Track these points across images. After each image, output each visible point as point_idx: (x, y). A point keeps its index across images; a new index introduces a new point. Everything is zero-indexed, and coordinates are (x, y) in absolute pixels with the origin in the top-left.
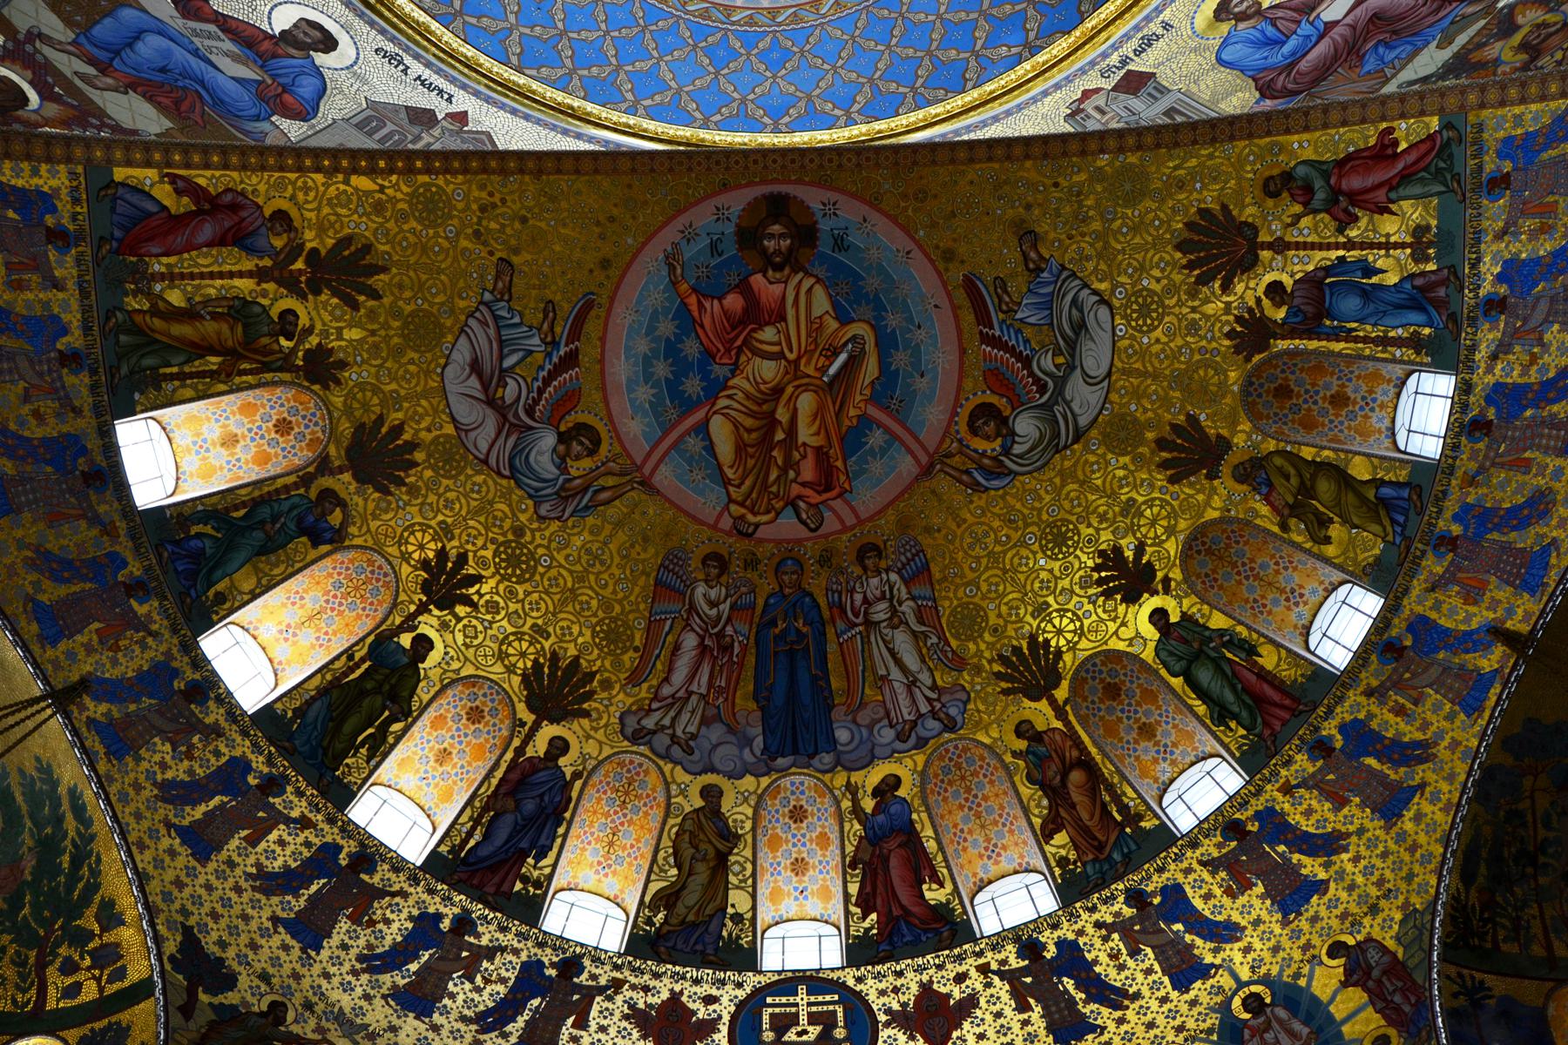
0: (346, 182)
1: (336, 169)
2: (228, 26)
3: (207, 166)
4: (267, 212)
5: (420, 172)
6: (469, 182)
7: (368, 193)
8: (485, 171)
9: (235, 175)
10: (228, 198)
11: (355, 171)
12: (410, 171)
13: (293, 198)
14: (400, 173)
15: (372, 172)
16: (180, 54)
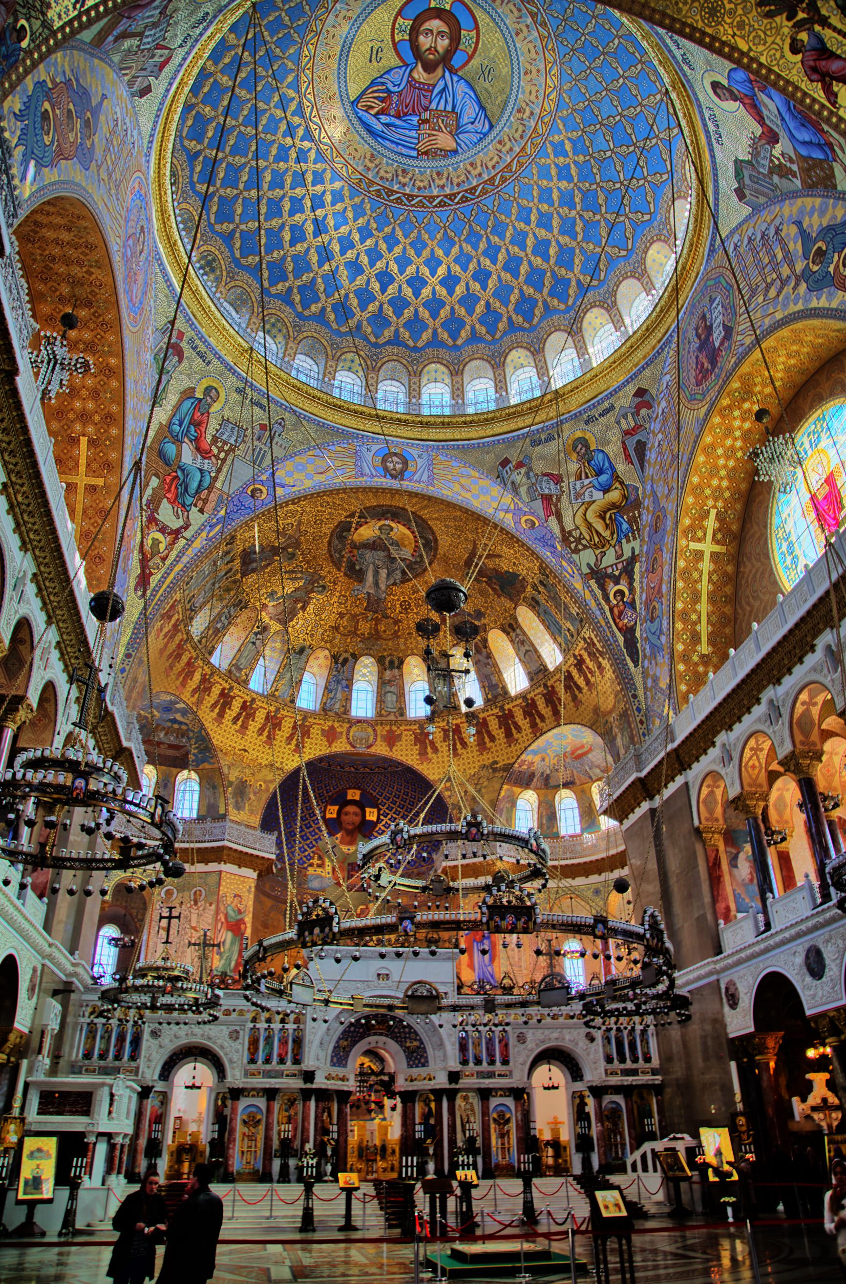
0: (750, 49)
1: (752, 60)
2: (760, 120)
3: (814, 100)
4: (800, 56)
5: (709, 35)
6: (685, 17)
7: (743, 37)
8: (674, 20)
9: (803, 87)
10: (814, 77)
11: (742, 54)
12: (714, 38)
13: (782, 57)
14: (719, 40)
15: (734, 48)
16: (791, 125)
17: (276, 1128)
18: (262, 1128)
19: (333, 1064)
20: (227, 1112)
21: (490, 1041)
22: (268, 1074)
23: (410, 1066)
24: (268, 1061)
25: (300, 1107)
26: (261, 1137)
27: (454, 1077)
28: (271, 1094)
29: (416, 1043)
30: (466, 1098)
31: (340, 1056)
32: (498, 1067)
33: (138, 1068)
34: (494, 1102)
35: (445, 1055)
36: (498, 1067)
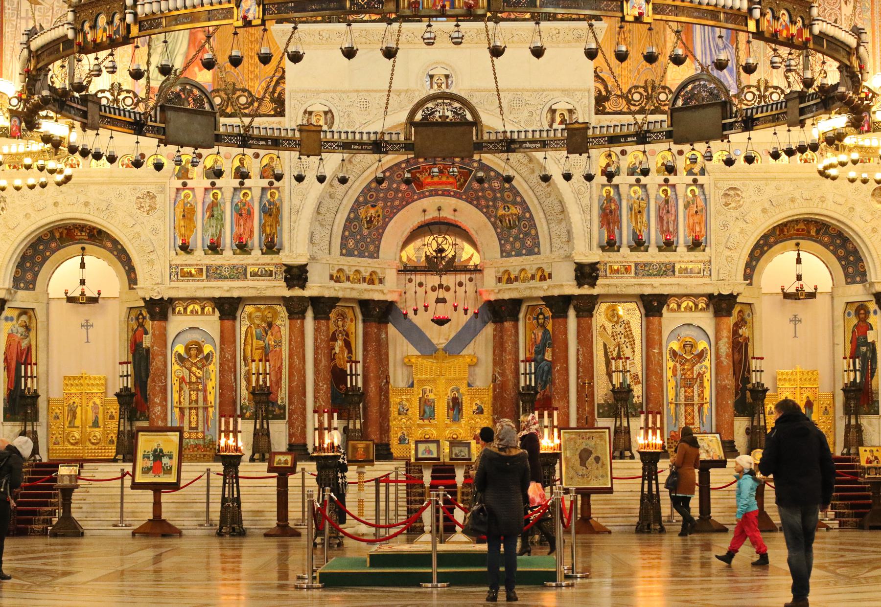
17: (241, 369)
18: (214, 368)
19: (346, 251)
20: (147, 341)
21: (666, 207)
22: (214, 273)
23: (505, 254)
24: (214, 248)
25: (285, 332)
26: (213, 385)
27: (586, 273)
28: (227, 308)
29: (515, 210)
30: (613, 316)
31: (361, 235)
32: (681, 256)
34: (670, 320)
35: (569, 232)
36: (681, 256)
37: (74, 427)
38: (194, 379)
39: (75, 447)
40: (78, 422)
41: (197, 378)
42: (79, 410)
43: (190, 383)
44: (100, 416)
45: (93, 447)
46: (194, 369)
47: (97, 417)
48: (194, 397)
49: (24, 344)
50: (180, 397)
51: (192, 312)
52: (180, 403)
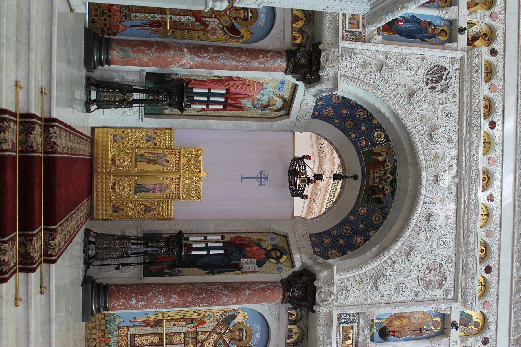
20: (248, 263)
33: (361, 38)
37: (136, 161)
38: (200, 337)
39: (110, 161)
40: (143, 166)
41: (203, 342)
42: (157, 167)
43: (197, 333)
44: (150, 194)
45: (110, 186)
46: (215, 337)
47: (148, 190)
48: (176, 339)
49: (247, 103)
50: (176, 320)
51: (290, 331)
52: (169, 321)
